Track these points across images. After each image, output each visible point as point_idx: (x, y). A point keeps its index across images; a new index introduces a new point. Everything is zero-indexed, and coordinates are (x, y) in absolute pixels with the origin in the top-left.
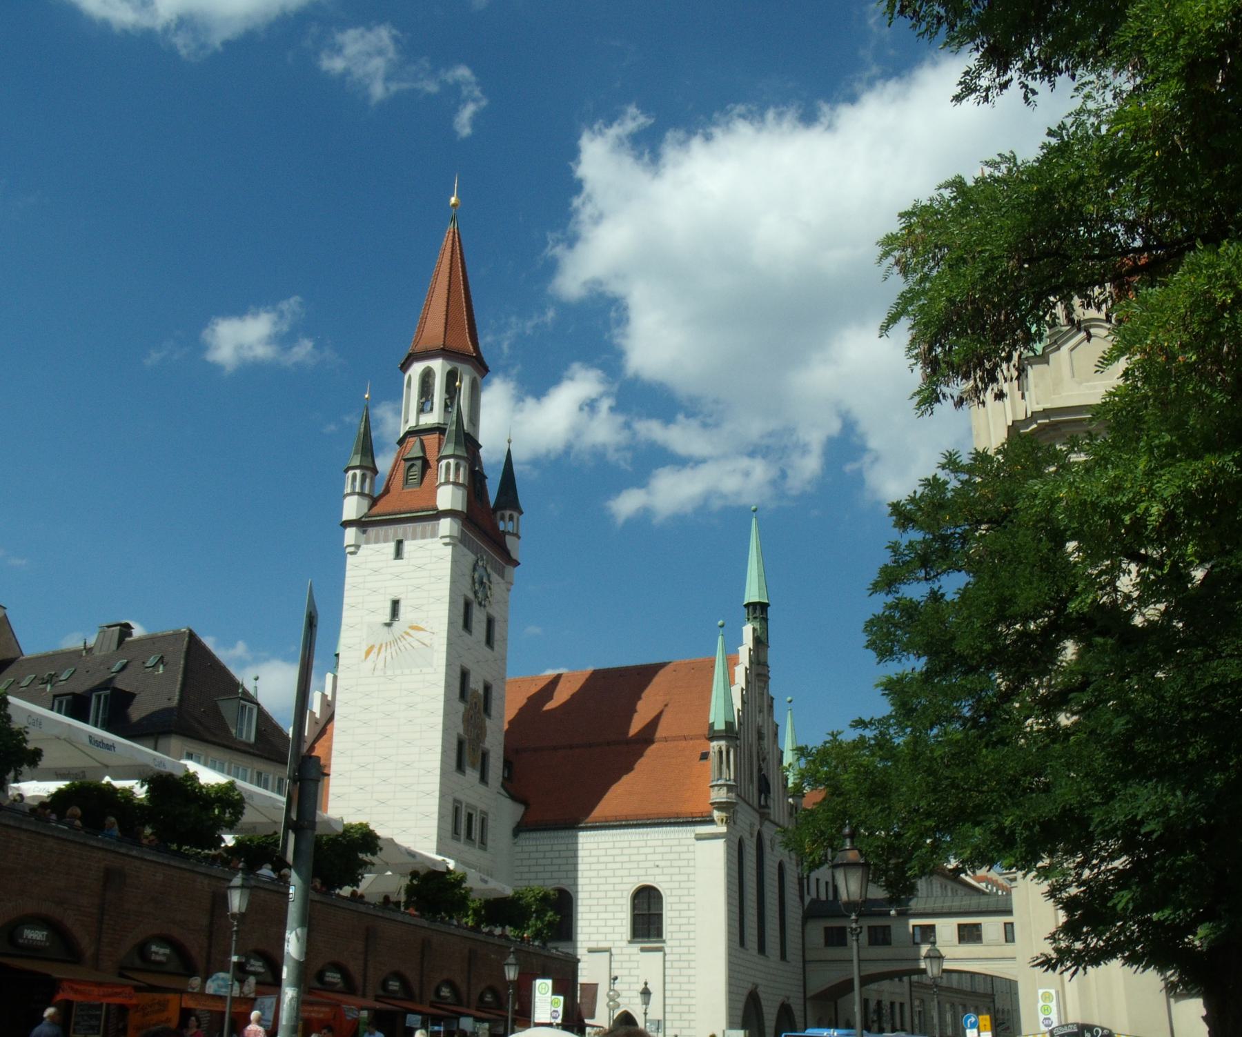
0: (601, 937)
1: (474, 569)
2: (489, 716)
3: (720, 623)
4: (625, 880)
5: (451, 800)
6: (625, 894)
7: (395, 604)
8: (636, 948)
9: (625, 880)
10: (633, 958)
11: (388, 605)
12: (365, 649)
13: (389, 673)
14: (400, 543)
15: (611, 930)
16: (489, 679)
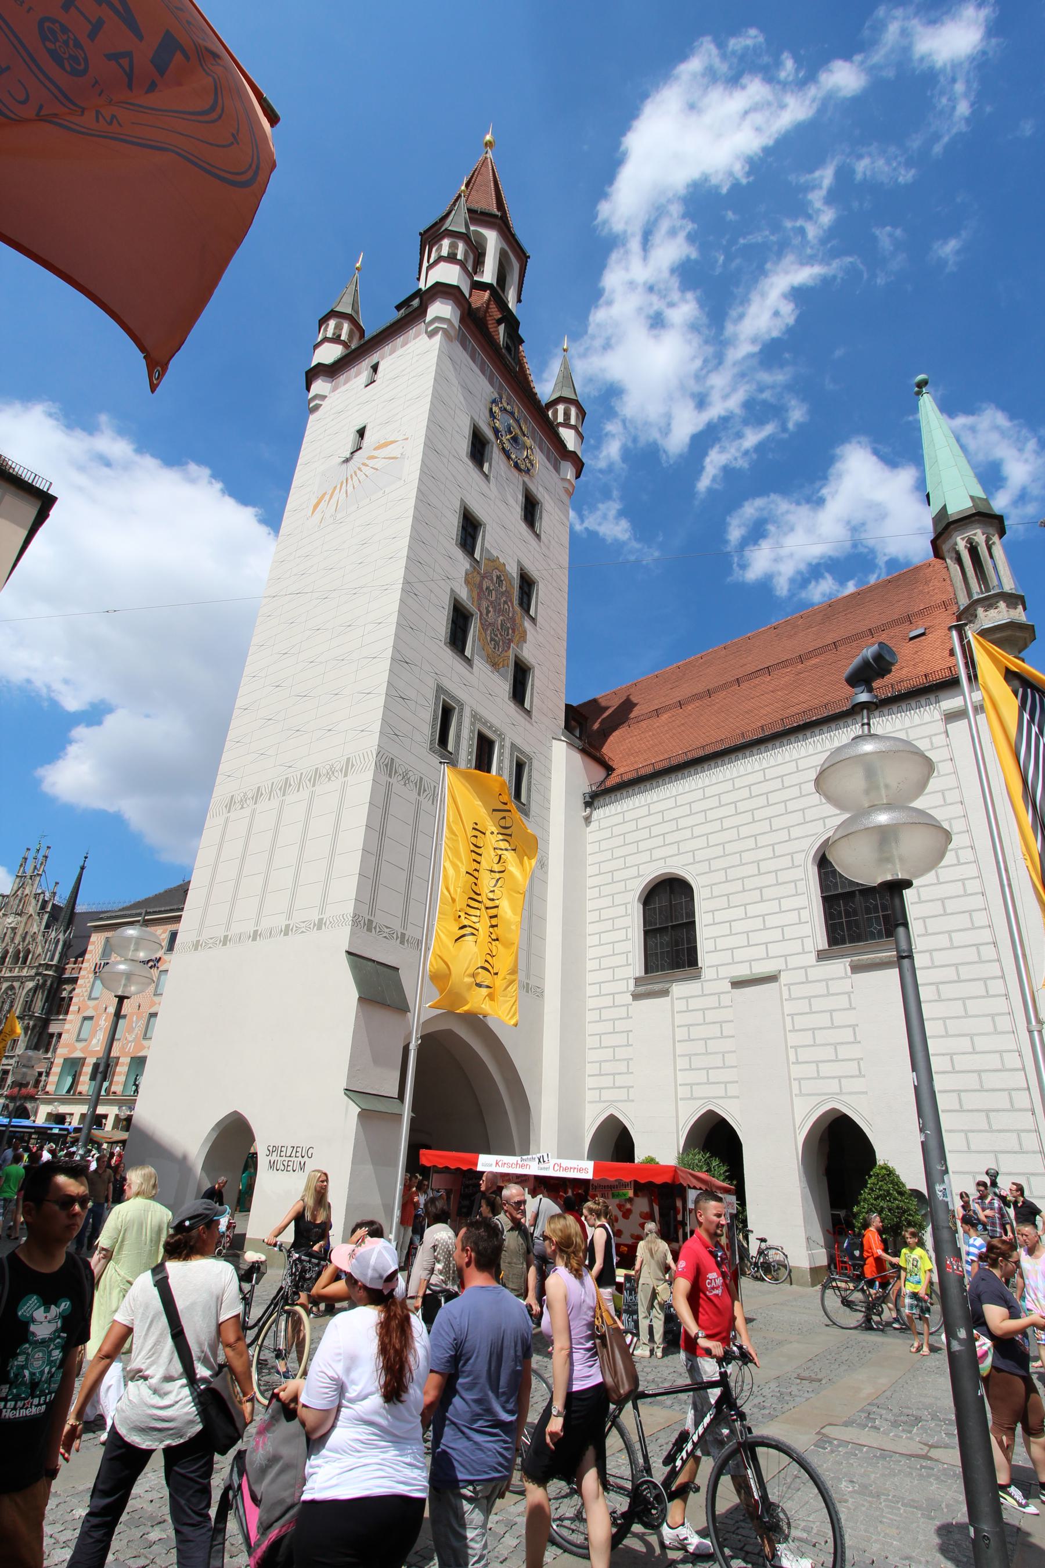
0: (760, 952)
1: (494, 401)
2: (533, 620)
3: (921, 377)
4: (796, 832)
5: (432, 685)
6: (799, 858)
7: (361, 433)
8: (840, 967)
9: (796, 832)
10: (835, 987)
11: (351, 437)
12: (314, 501)
13: (339, 516)
14: (375, 368)
15: (777, 935)
16: (534, 572)
